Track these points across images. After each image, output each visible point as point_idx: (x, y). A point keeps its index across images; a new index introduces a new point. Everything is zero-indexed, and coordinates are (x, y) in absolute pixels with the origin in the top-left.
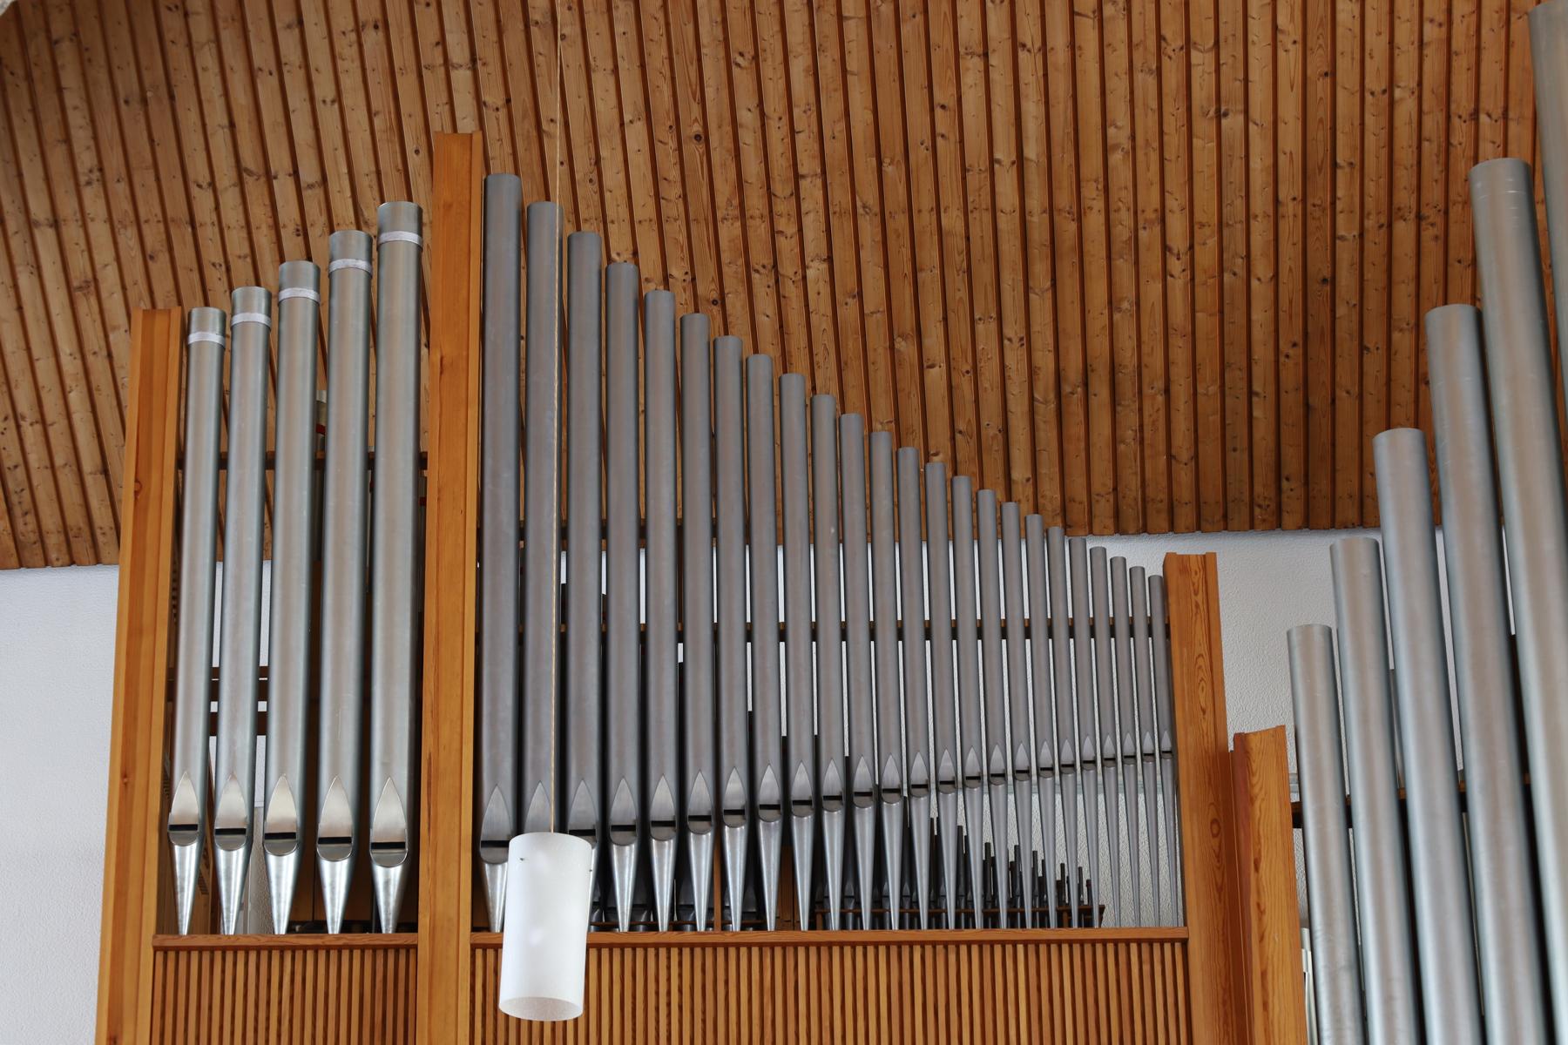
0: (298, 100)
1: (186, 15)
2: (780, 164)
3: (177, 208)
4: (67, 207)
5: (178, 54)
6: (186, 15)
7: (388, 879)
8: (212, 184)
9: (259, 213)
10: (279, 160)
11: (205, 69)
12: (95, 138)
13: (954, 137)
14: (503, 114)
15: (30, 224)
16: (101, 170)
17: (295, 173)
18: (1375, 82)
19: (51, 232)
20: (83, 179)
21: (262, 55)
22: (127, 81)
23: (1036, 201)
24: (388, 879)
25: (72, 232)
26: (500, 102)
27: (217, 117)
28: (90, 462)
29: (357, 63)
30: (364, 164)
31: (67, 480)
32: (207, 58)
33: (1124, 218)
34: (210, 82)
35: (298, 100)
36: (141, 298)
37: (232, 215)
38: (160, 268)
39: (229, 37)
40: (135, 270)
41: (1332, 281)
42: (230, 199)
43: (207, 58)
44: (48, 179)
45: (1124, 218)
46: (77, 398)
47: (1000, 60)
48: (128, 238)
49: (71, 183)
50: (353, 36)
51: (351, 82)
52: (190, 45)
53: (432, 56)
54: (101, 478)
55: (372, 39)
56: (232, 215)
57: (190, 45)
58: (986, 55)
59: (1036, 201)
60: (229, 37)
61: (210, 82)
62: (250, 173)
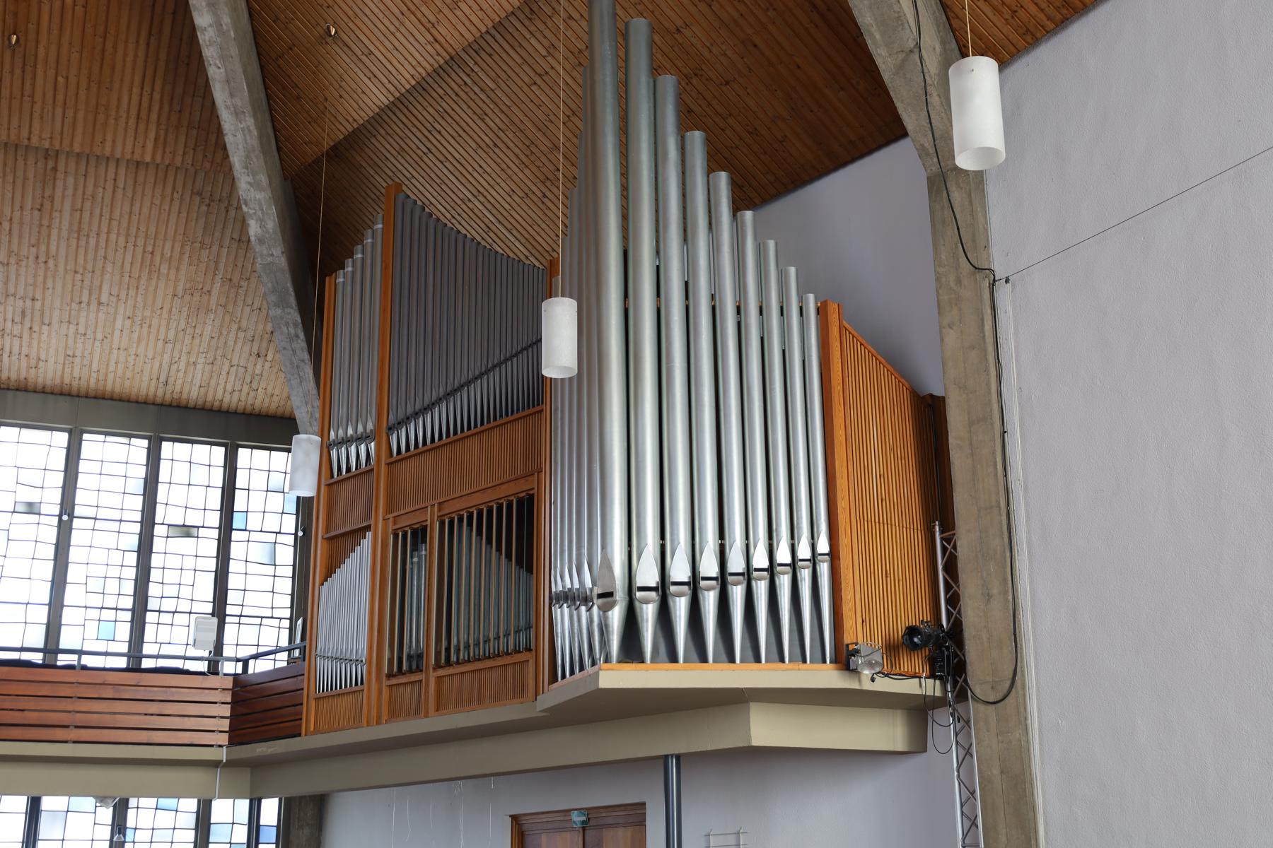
2: (520, 145)
32: (377, 177)
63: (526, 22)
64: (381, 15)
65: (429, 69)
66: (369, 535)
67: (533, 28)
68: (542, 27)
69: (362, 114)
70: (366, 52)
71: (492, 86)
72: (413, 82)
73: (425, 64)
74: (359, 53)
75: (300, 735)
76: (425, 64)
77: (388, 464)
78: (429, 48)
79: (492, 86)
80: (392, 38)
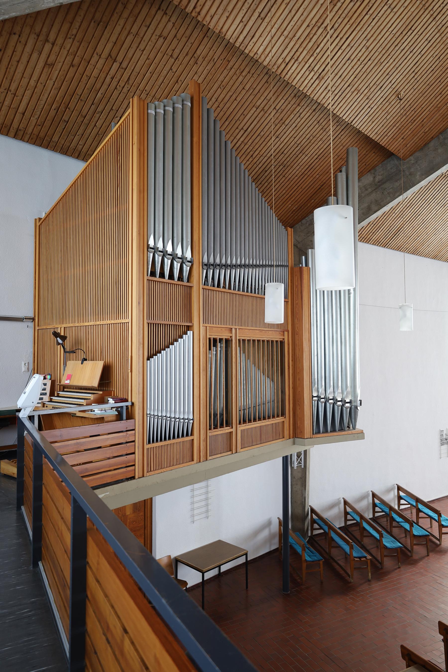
0: (134, 46)
1: (125, 7)
3: (87, 57)
4: (60, 41)
5: (115, 16)
6: (125, 7)
7: (186, 269)
8: (100, 55)
9: (106, 68)
10: (120, 58)
11: (119, 25)
12: (80, 27)
13: (241, 121)
14: (173, 74)
15: (47, 40)
16: (75, 36)
17: (121, 64)
18: (298, 142)
19: (51, 45)
20: (69, 36)
21: (134, 30)
22: (98, 16)
23: (242, 139)
24: (186, 269)
25: (56, 49)
26: (175, 71)
27: (113, 39)
28: (21, 109)
29: (154, 44)
30: (137, 69)
31: (12, 112)
32: (122, 22)
33: (251, 148)
34: (118, 28)
35: (134, 46)
36: (63, 75)
37: (99, 66)
38: (72, 70)
39: (131, 20)
40: (66, 67)
41: (266, 171)
42: (101, 61)
43: (122, 22)
44: (59, 31)
45: (251, 148)
46: (28, 93)
47: (259, 110)
48: (69, 58)
49: (65, 36)
50: (157, 37)
51: (149, 48)
52: (120, 16)
53: (169, 52)
54: (22, 115)
55: (161, 40)
56: (99, 66)
57: (120, 16)
58: (257, 109)
59: (242, 139)
60: (131, 20)
61: (118, 28)
62: (111, 57)
63: (293, 95)
64: (292, 23)
65: (265, 63)
66: (190, 333)
67: (290, 99)
68: (292, 103)
69: (208, 18)
70: (263, 15)
71: (247, 87)
72: (252, 54)
73: (268, 60)
74: (259, 10)
75: (133, 478)
76: (268, 60)
77: (203, 289)
78: (280, 60)
79: (247, 87)
80: (279, 33)
